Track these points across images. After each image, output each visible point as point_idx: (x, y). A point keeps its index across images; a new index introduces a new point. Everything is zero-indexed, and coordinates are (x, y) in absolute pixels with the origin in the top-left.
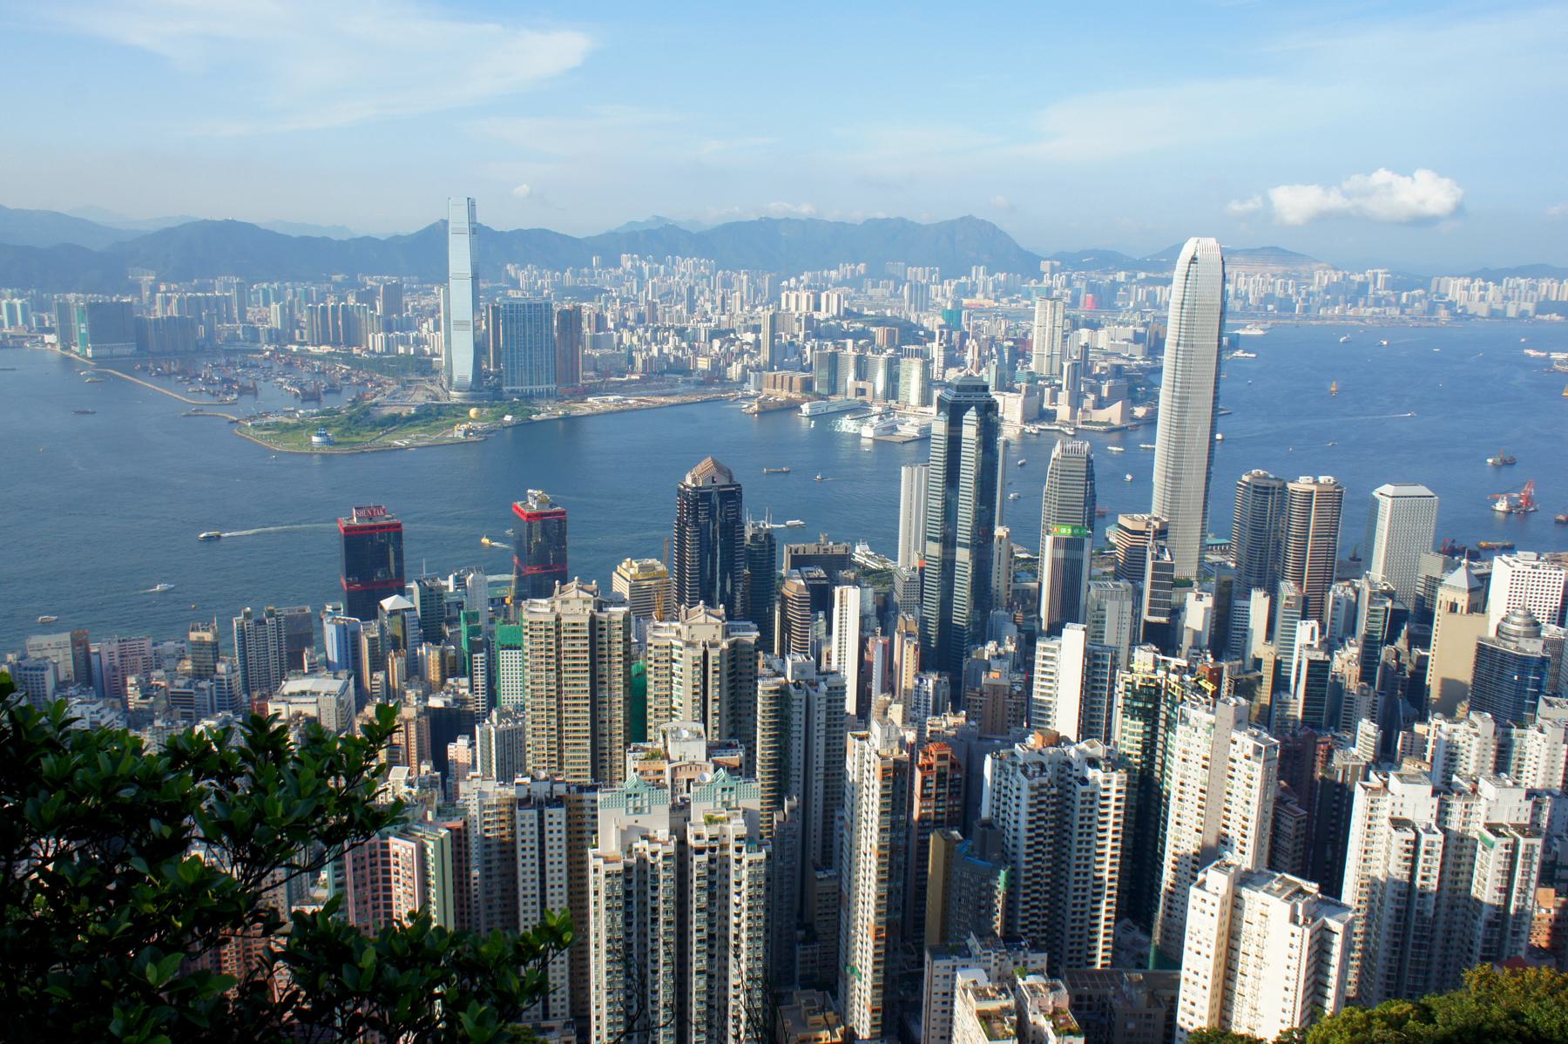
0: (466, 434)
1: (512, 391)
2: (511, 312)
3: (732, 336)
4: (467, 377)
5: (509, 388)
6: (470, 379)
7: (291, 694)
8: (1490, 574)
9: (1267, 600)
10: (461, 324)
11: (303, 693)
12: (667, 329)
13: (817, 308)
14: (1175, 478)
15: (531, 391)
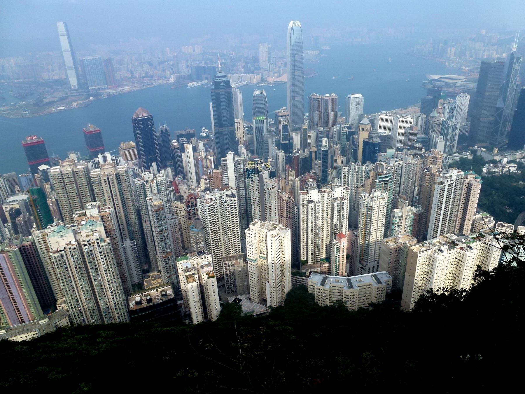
0: (77, 105)
1: (92, 89)
2: (87, 62)
3: (166, 63)
4: (75, 86)
5: (91, 88)
6: (77, 87)
7: (10, 202)
8: (375, 119)
9: (315, 133)
10: (70, 68)
11: (14, 201)
12: (144, 63)
13: (194, 51)
14: (293, 98)
15: (99, 88)
